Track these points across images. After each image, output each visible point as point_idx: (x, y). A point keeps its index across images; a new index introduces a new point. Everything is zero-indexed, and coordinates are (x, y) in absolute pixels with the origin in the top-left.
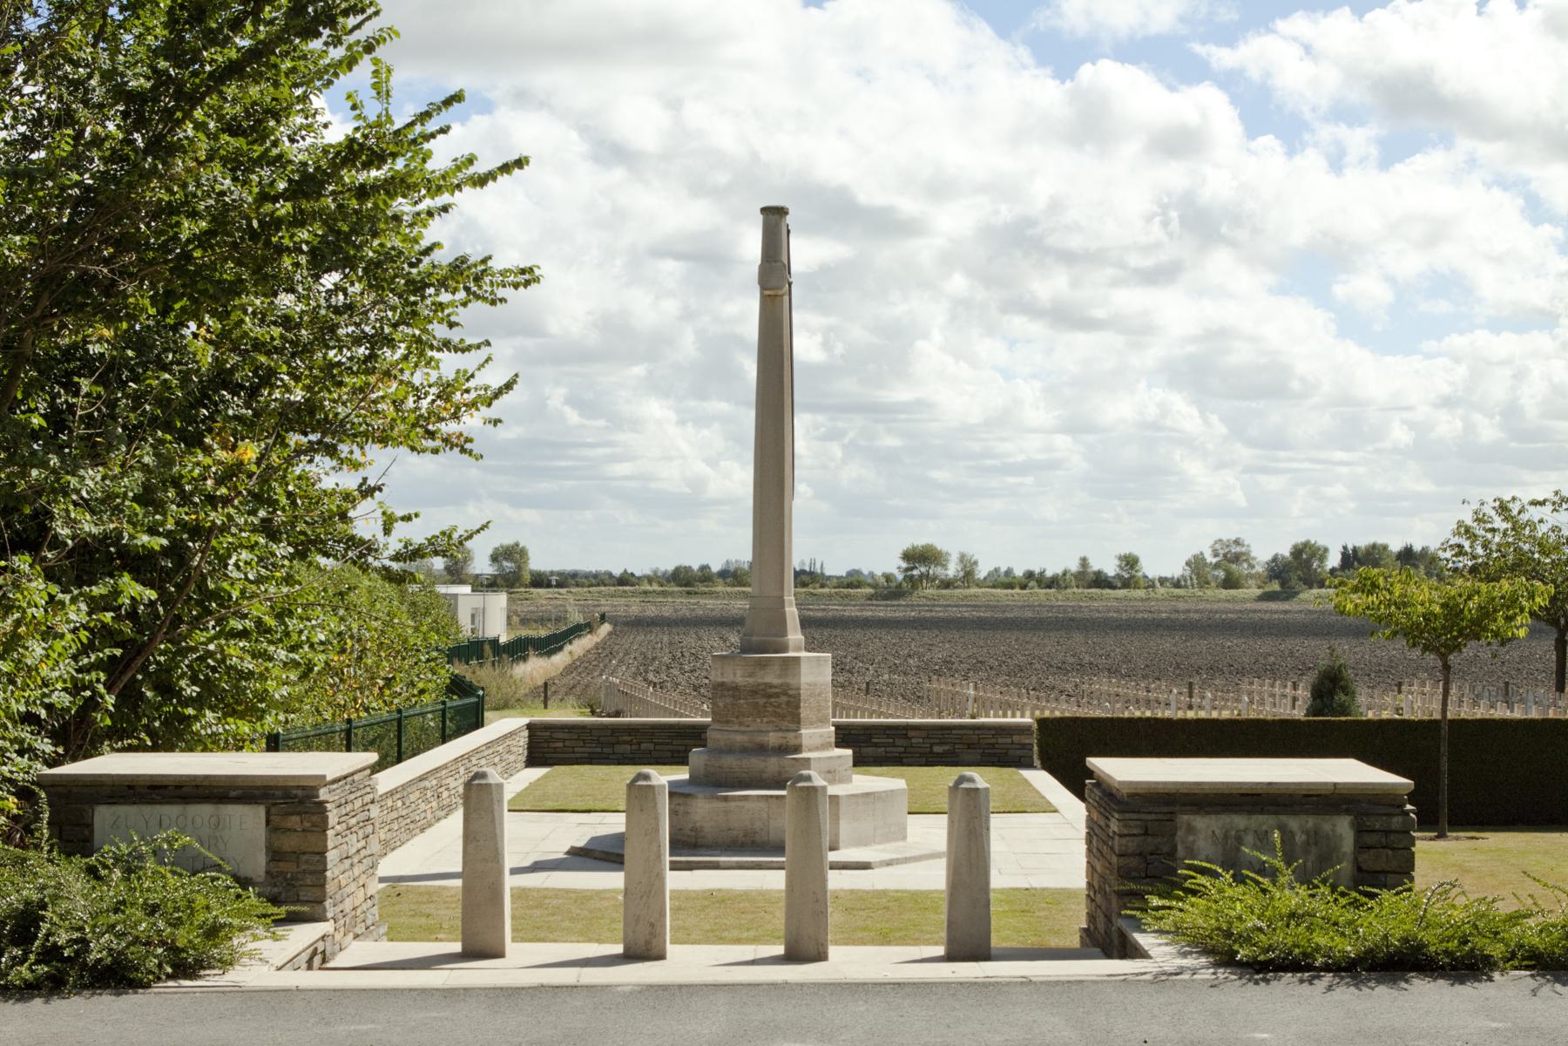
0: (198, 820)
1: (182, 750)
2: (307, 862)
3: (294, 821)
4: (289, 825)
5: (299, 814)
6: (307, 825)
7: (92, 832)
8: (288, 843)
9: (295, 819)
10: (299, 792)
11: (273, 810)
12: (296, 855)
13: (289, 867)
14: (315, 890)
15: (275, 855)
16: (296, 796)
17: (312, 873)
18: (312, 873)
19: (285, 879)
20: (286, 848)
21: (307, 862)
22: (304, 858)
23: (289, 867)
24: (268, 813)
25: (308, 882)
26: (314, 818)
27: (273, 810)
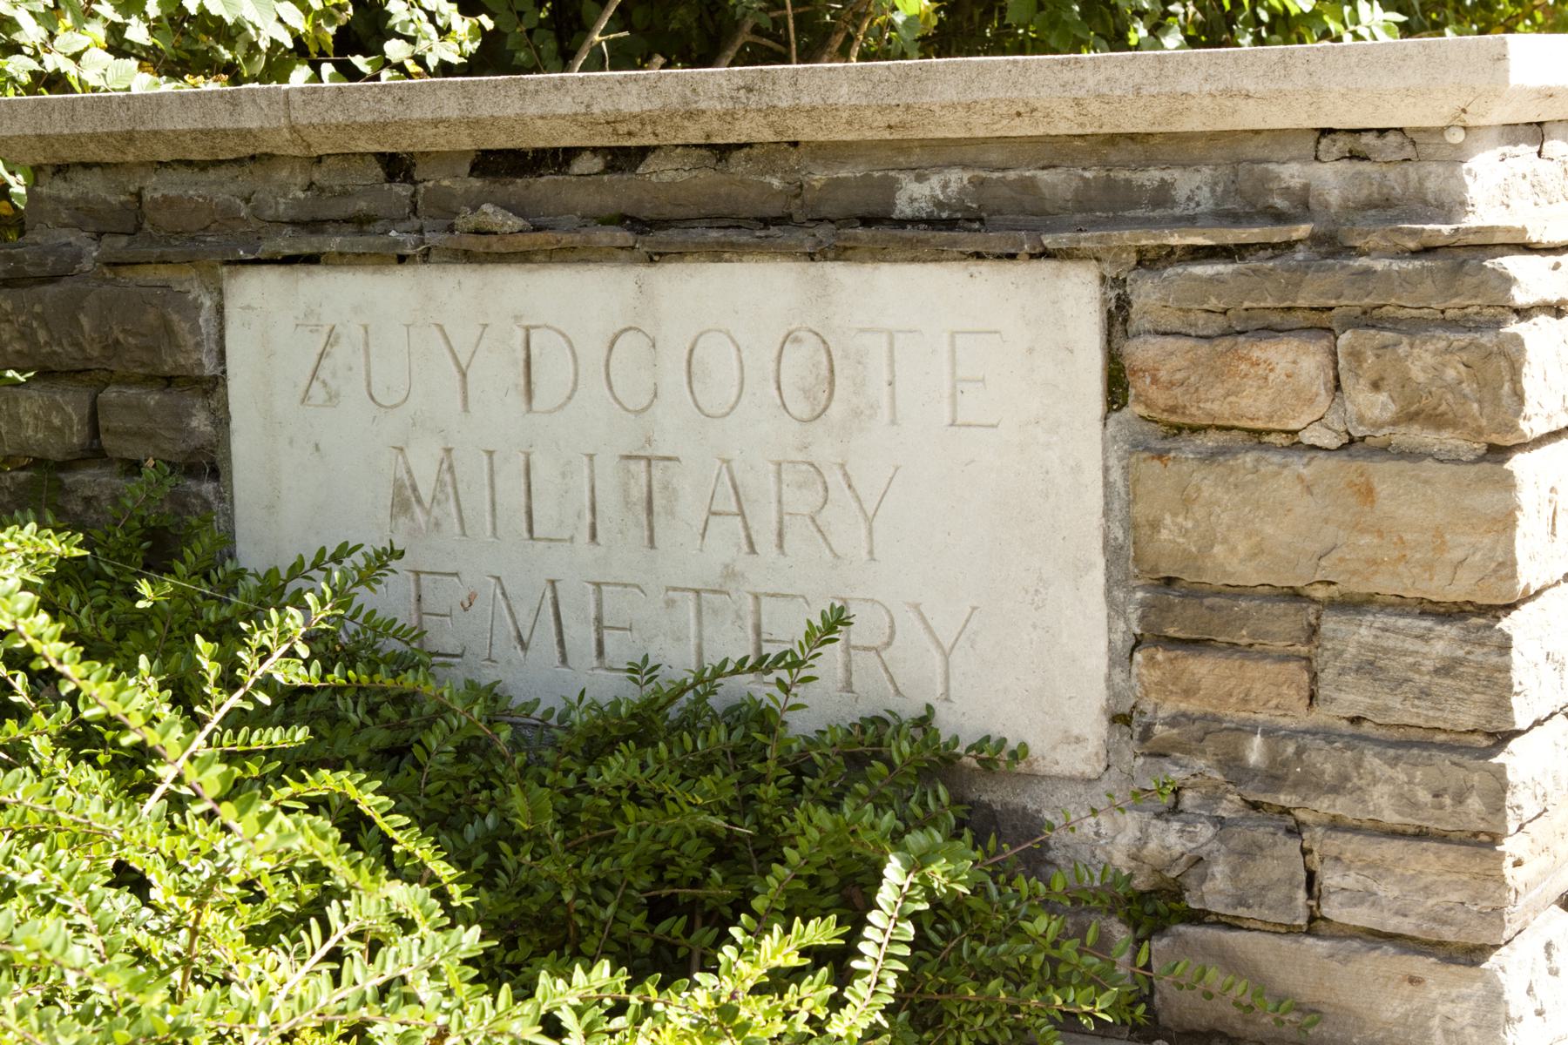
0: (717, 358)
1: (1540, 28)
2: (1369, 668)
3: (1283, 377)
4: (1252, 405)
5: (1319, 325)
6: (1371, 406)
7: (222, 421)
8: (1253, 527)
9: (1294, 363)
10: (1331, 179)
11: (1147, 294)
12: (1308, 608)
13: (1251, 692)
14: (1428, 861)
15: (1171, 610)
16: (1303, 204)
17: (1410, 743)
18: (1410, 743)
19: (1233, 767)
20: (1233, 562)
21: (1369, 668)
22: (1353, 636)
23: (1251, 692)
24: (1117, 317)
25: (1383, 806)
26: (1422, 360)
27: (1147, 294)
